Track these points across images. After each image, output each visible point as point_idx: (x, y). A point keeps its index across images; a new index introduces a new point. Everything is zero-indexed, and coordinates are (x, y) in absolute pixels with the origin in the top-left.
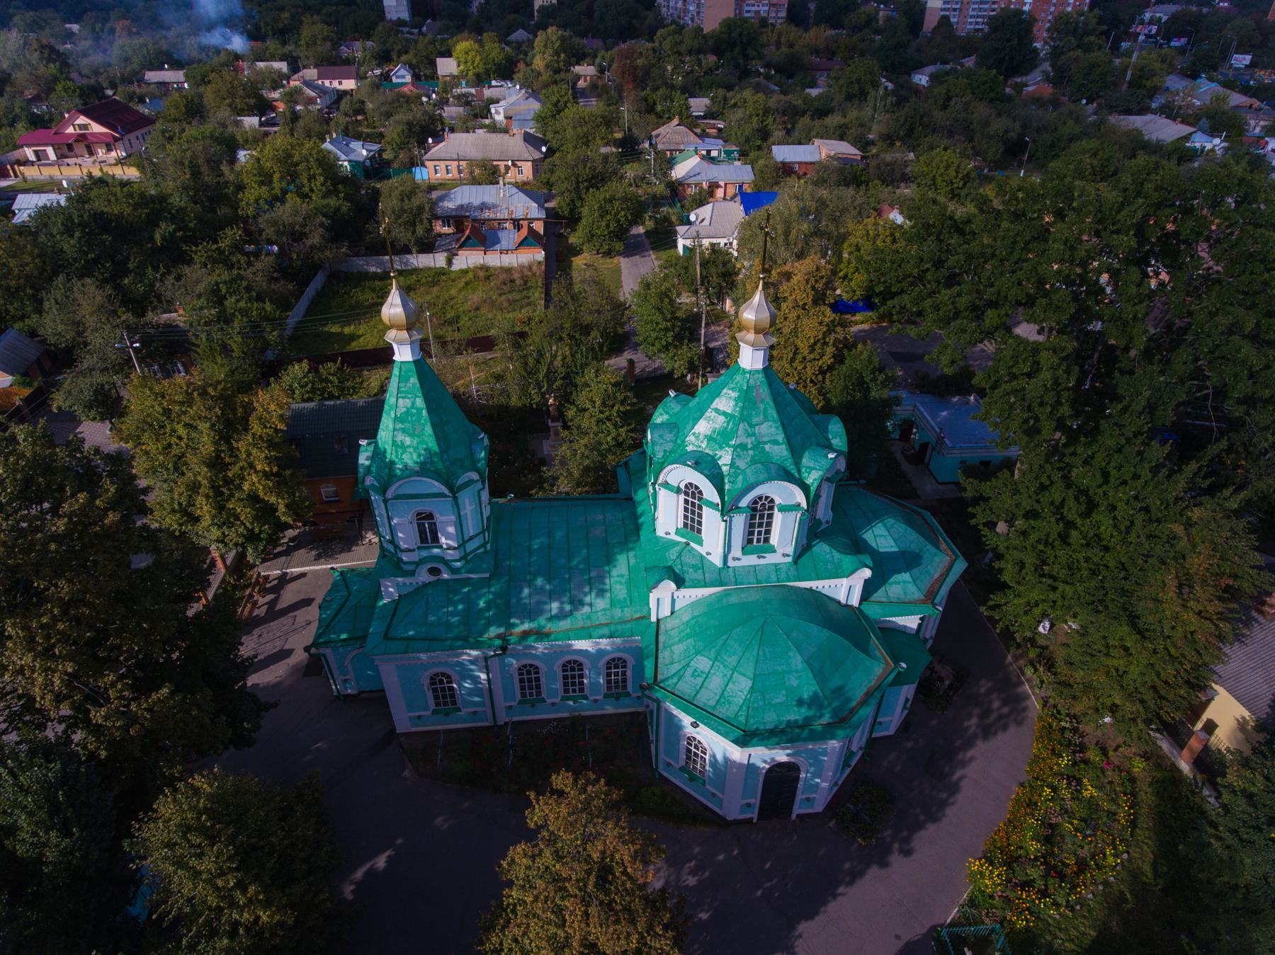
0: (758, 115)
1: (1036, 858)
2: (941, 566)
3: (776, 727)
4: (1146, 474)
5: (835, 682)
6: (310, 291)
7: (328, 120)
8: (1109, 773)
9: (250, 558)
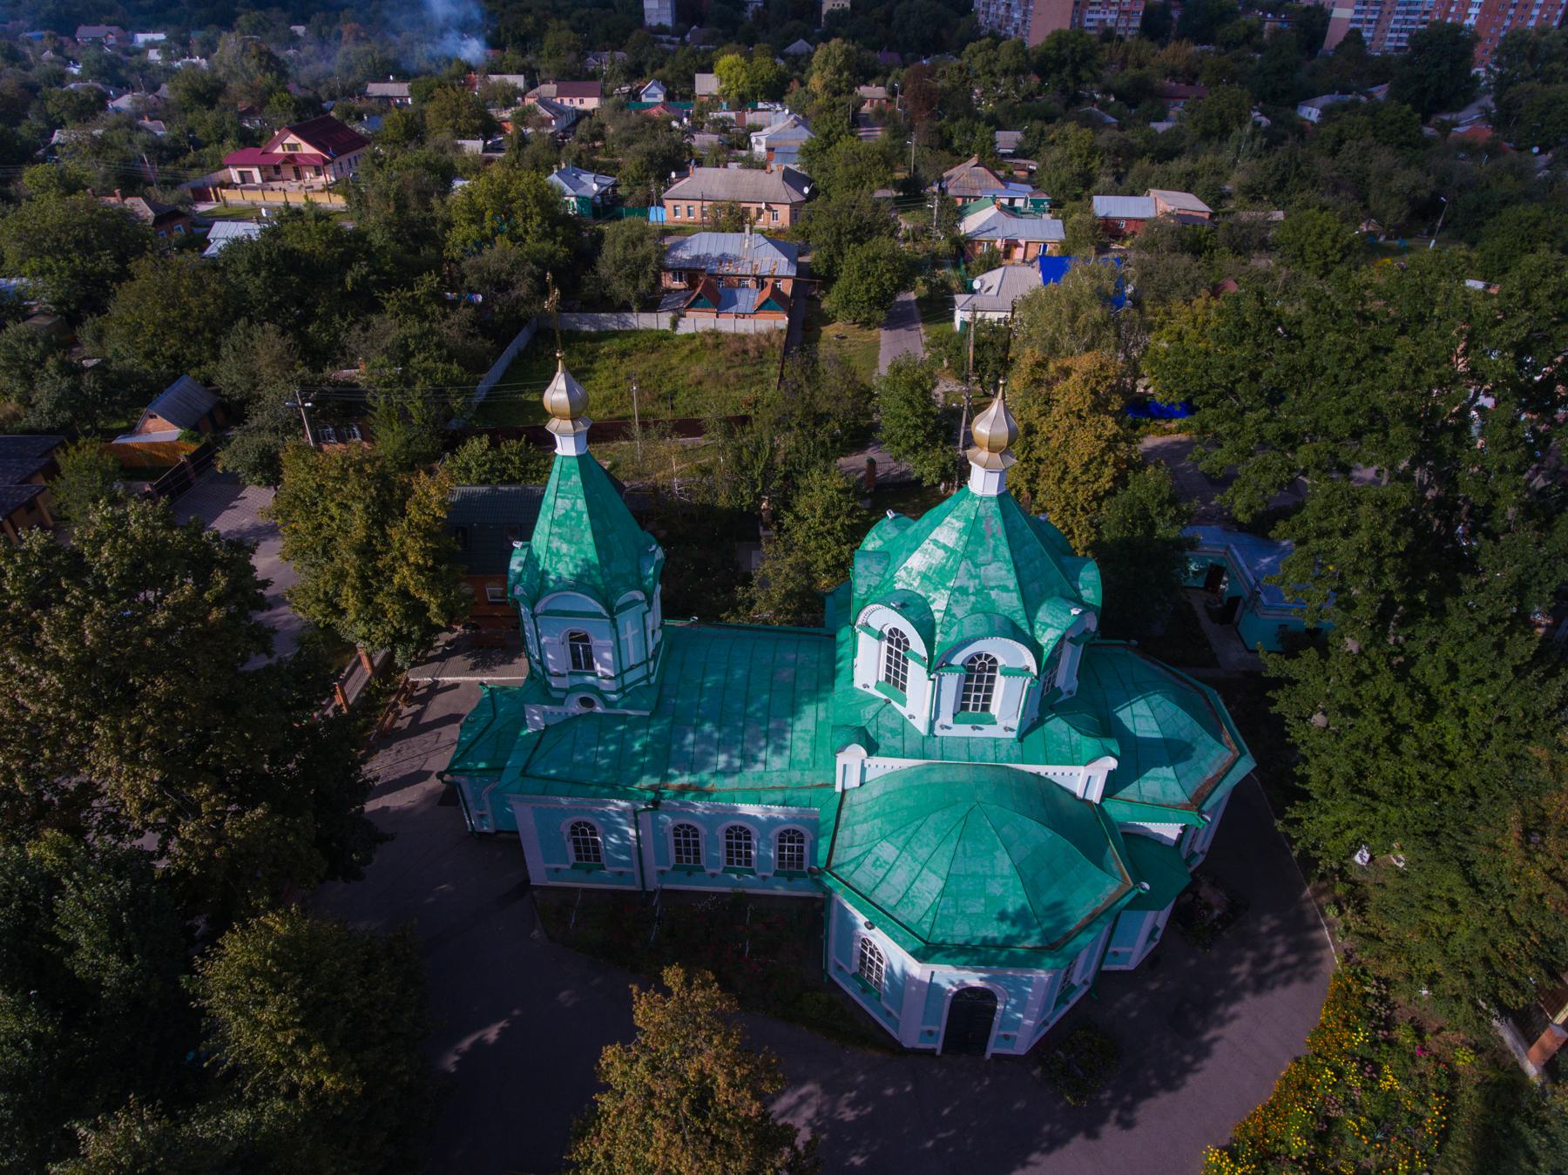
0: (1080, 156)
1: (1299, 1160)
2: (1219, 763)
3: (967, 943)
4: (1507, 674)
5: (1052, 896)
6: (511, 351)
7: (559, 147)
8: (1422, 1062)
9: (398, 661)
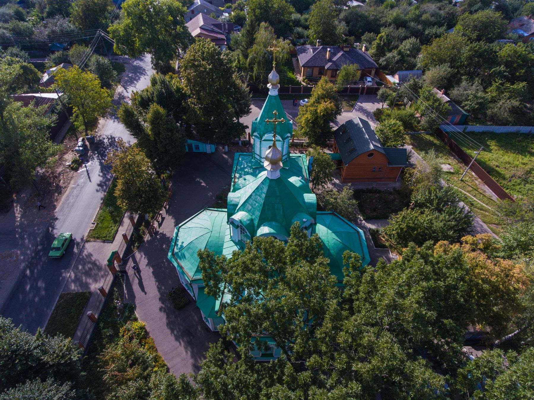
5: (187, 255)
